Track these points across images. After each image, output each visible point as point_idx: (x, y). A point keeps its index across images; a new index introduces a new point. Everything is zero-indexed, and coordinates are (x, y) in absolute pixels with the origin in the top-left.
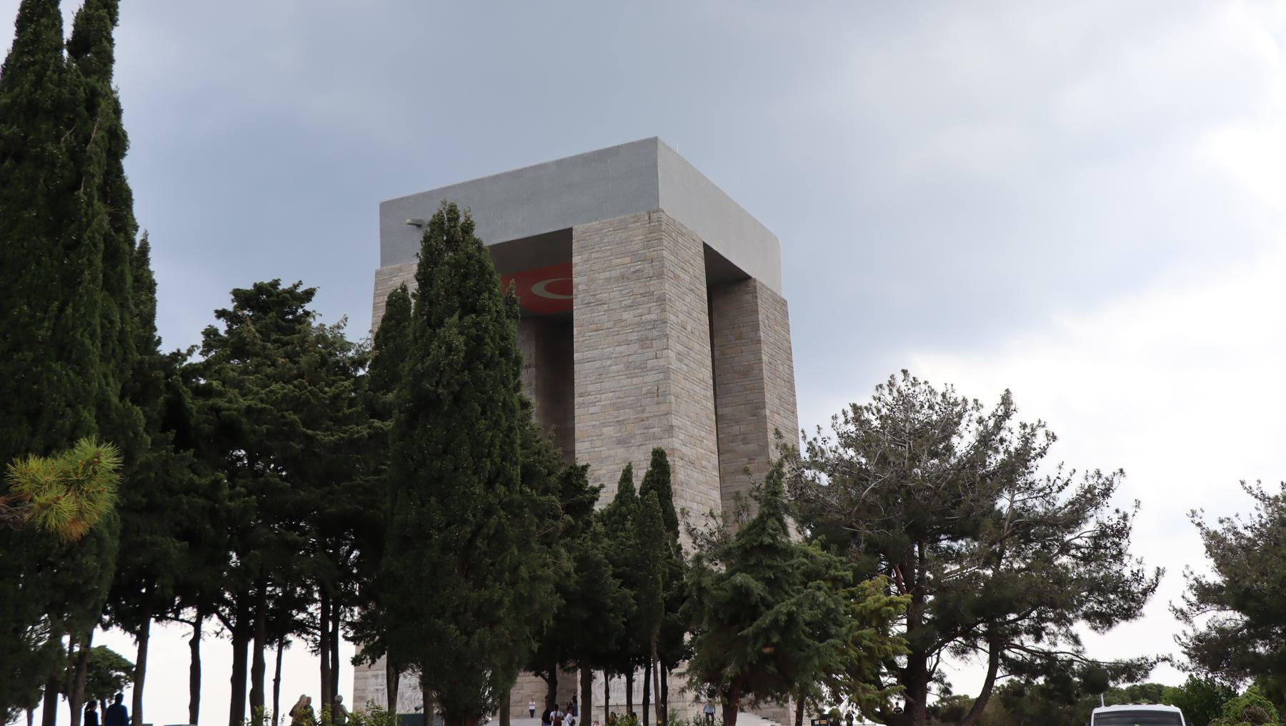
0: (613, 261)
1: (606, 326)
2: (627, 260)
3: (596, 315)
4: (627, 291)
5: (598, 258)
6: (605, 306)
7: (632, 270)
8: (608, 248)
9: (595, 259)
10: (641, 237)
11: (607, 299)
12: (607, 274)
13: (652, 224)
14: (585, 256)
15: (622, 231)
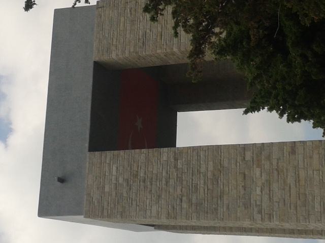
0: (121, 29)
1: (160, 29)
2: (122, 19)
3: (151, 35)
4: (141, 17)
5: (117, 40)
6: (148, 31)
7: (129, 15)
8: (112, 33)
9: (116, 42)
10: (111, 12)
11: (143, 30)
12: (128, 32)
13: (105, 5)
14: (113, 48)
15: (104, 25)
